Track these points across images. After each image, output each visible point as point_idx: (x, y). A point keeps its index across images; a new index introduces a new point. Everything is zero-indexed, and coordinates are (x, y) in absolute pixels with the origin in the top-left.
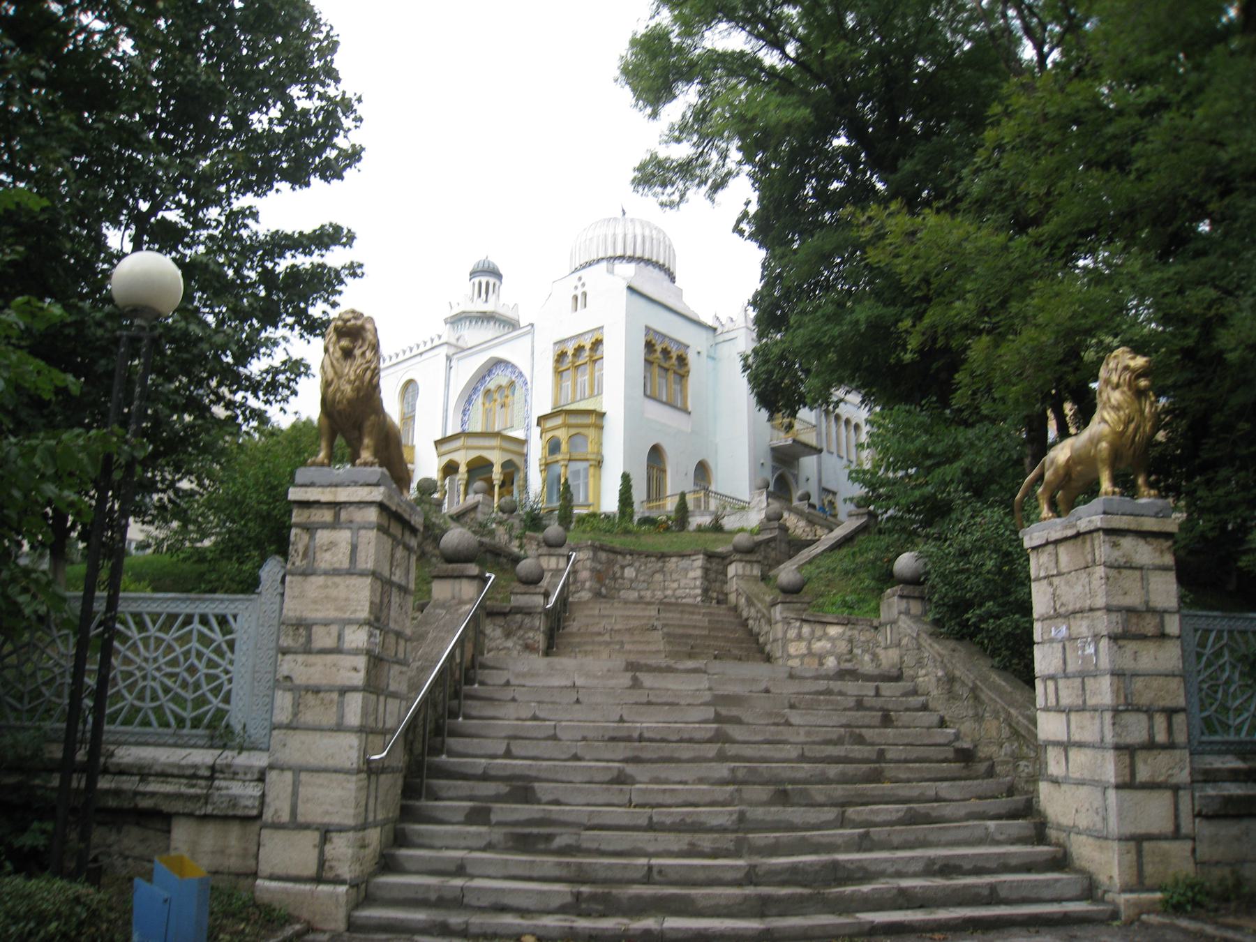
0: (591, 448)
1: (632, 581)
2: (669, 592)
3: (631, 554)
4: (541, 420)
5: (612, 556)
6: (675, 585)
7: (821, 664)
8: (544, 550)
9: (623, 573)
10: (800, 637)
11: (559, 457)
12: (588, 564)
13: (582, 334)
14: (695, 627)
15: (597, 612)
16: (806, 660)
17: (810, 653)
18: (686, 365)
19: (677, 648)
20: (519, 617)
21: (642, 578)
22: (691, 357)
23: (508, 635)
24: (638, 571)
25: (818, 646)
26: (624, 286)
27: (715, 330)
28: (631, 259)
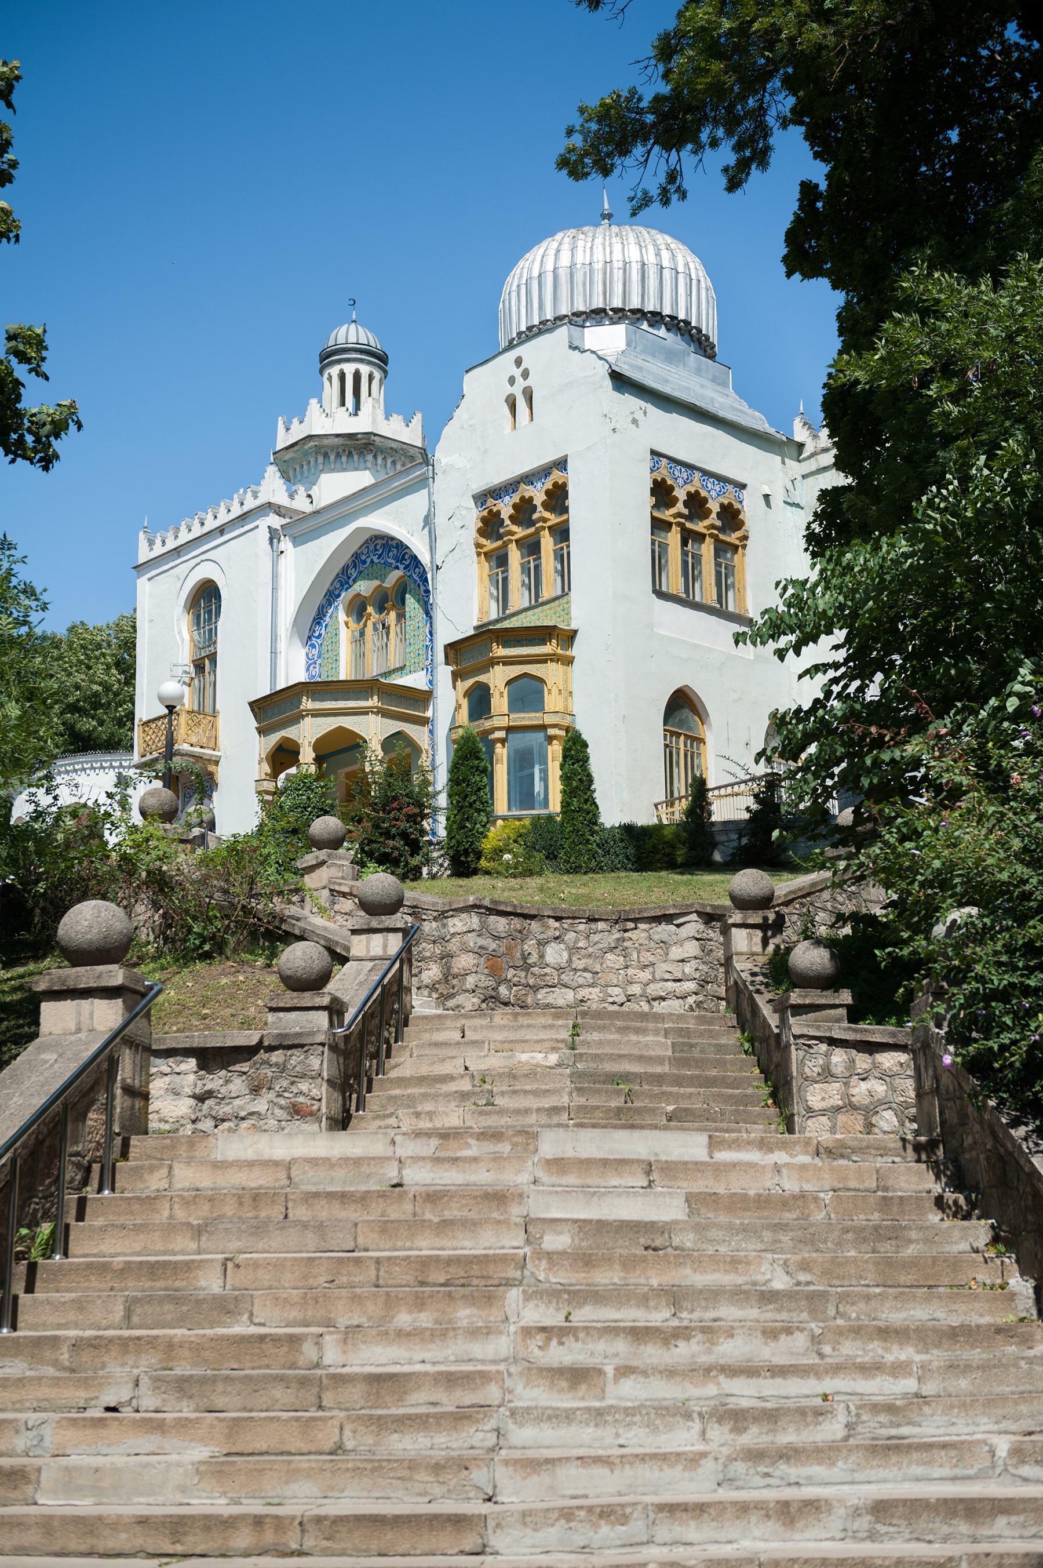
0: (552, 701)
1: (560, 969)
2: (636, 989)
3: (558, 919)
4: (454, 650)
5: (517, 923)
6: (646, 975)
7: (869, 1127)
8: (361, 919)
9: (542, 956)
10: (827, 1074)
11: (487, 724)
12: (471, 940)
13: (528, 478)
14: (640, 1059)
15: (457, 1036)
16: (841, 1118)
17: (849, 1106)
19: (593, 1102)
20: (277, 1057)
22: (751, 508)
23: (255, 1090)
24: (573, 950)
25: (860, 1090)
26: (603, 370)
27: (801, 446)
28: (619, 315)
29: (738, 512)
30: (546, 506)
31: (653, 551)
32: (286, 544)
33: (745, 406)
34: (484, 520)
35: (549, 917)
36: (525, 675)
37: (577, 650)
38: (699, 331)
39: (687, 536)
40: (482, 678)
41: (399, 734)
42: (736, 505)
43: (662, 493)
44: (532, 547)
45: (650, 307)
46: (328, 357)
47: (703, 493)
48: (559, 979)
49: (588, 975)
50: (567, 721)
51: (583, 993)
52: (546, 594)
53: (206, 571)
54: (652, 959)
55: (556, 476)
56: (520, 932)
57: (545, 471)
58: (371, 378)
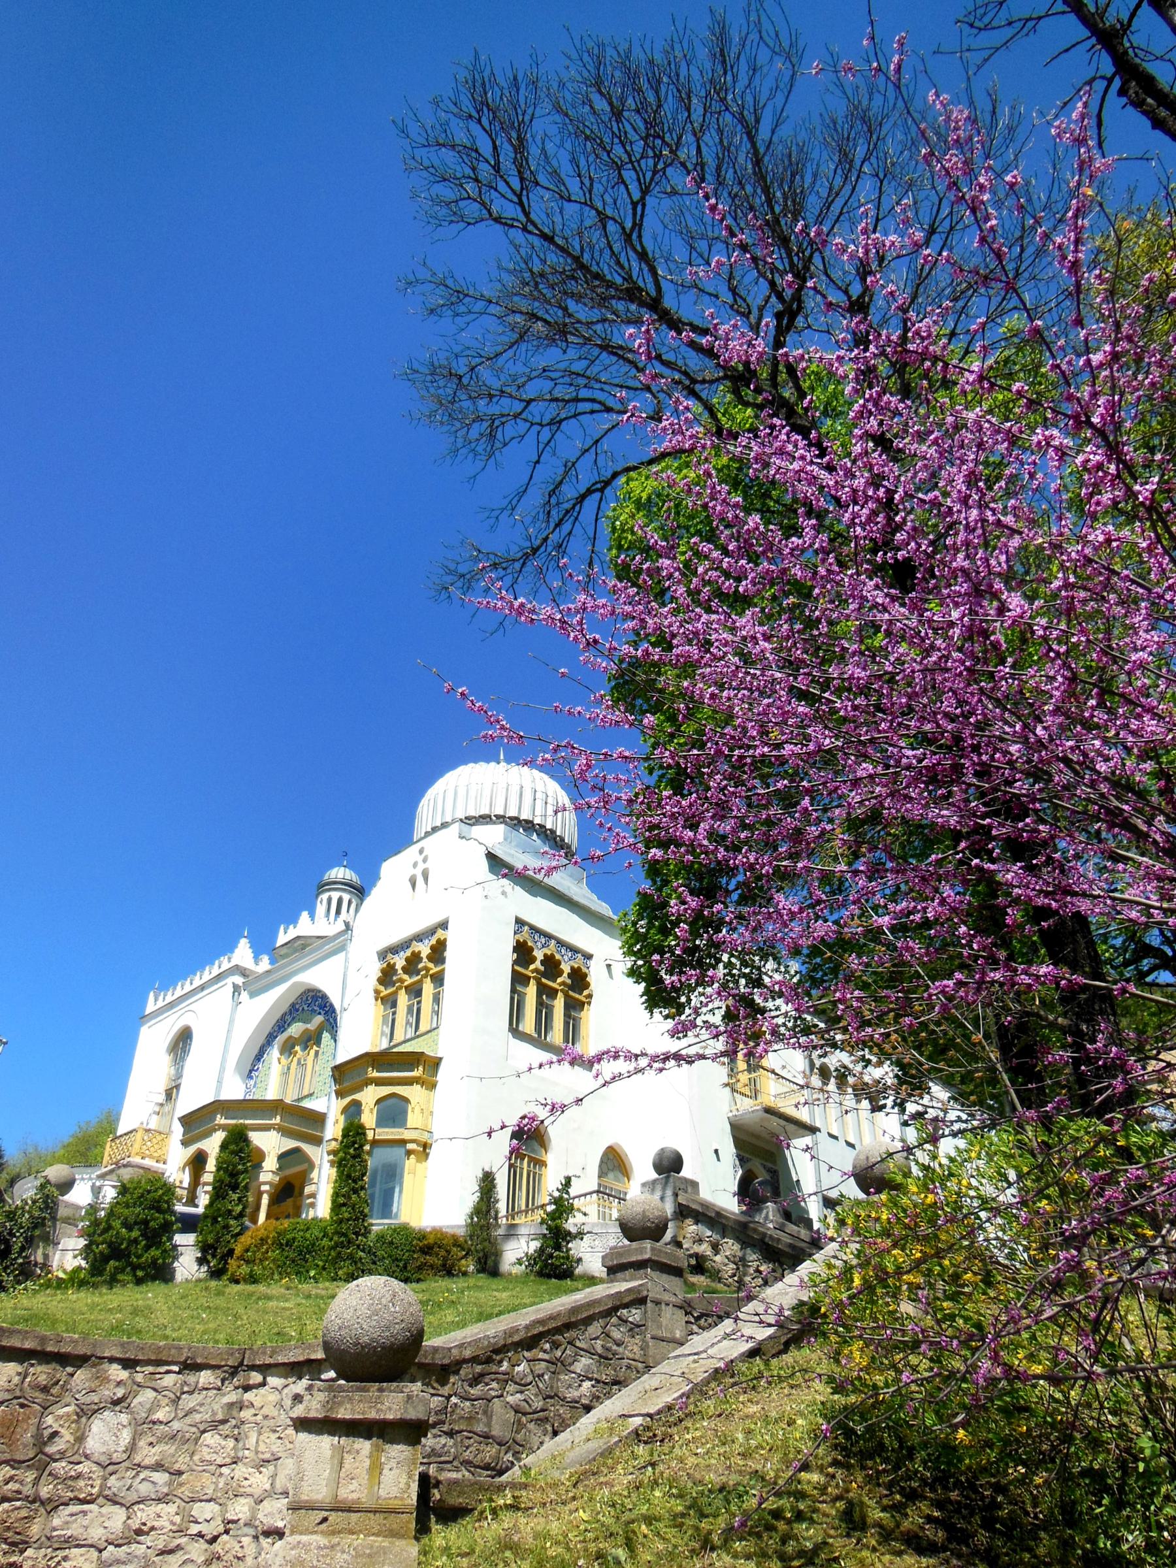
0: (413, 1119)
1: (109, 1466)
2: (240, 1509)
3: (128, 1364)
5: (41, 1373)
6: (259, 1481)
9: (80, 1439)
13: (419, 938)
18: (587, 986)
21: (147, 1454)
22: (596, 974)
24: (144, 1425)
29: (586, 975)
30: (430, 958)
31: (512, 999)
32: (244, 995)
33: (595, 897)
34: (383, 971)
35: (112, 1360)
36: (393, 1095)
37: (442, 1075)
38: (562, 840)
39: (542, 990)
40: (357, 1096)
41: (296, 1150)
42: (584, 970)
43: (523, 952)
44: (415, 992)
45: (523, 817)
46: (323, 887)
47: (558, 957)
48: (103, 1487)
49: (161, 1478)
50: (424, 1137)
51: (143, 1514)
52: (423, 1027)
53: (187, 1020)
54: (277, 1447)
55: (440, 934)
56: (45, 1389)
57: (432, 931)
58: (350, 902)
